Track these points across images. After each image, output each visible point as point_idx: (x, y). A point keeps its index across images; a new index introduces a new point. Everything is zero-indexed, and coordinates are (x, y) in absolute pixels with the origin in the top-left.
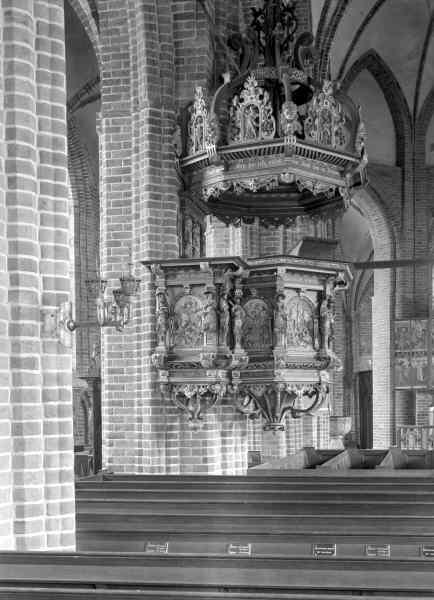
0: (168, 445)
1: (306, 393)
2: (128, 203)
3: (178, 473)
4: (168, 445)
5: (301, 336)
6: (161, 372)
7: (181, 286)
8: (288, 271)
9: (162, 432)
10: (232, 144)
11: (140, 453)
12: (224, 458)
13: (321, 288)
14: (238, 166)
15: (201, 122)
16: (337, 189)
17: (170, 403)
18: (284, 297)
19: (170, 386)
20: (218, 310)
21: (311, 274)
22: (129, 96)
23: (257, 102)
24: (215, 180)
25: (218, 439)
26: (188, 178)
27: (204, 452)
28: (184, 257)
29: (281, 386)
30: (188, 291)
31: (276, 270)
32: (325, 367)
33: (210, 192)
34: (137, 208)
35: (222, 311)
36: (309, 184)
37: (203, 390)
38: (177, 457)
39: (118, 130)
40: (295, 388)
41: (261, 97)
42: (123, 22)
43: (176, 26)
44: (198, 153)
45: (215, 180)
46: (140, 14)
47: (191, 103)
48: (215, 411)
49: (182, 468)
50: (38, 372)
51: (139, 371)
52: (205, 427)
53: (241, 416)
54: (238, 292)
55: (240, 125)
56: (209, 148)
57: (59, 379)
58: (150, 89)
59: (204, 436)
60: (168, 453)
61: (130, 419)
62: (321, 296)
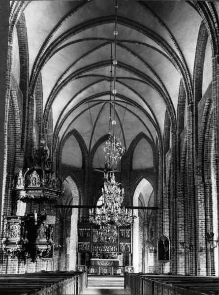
5: (44, 236)
6: (4, 245)
12: (18, 270)
14: (30, 192)
23: (36, 177)
24: (23, 194)
33: (21, 197)
36: (48, 197)
45: (23, 194)
56: (22, 187)
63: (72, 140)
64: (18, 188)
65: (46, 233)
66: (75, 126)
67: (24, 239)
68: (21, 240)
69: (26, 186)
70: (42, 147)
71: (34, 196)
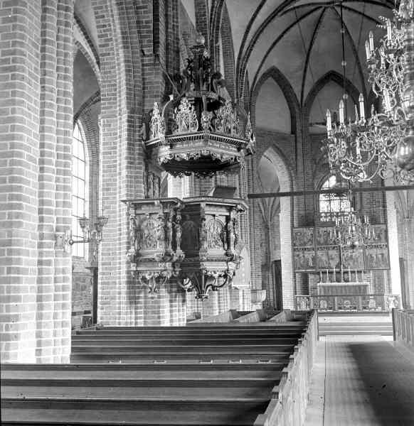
0: (136, 308)
1: (220, 276)
2: (115, 166)
3: (142, 326)
4: (136, 308)
5: (216, 242)
6: (132, 264)
7: (144, 214)
8: (207, 204)
9: (133, 300)
10: (174, 135)
11: (120, 313)
12: (171, 316)
13: (228, 214)
14: (178, 146)
15: (157, 121)
16: (235, 159)
17: (136, 284)
18: (205, 220)
19: (137, 273)
20: (166, 229)
21: (221, 206)
22: (116, 108)
24: (165, 153)
25: (168, 304)
26: (149, 153)
27: (159, 313)
28: (147, 197)
29: (204, 272)
30: (148, 217)
31: (200, 205)
32: (231, 260)
33: (162, 160)
34: (120, 169)
35: (168, 228)
36: (219, 156)
37: (156, 275)
38: (143, 315)
39: (110, 125)
40: (213, 273)
41: (190, 109)
42: (114, 67)
43: (143, 70)
44: (156, 138)
45: (165, 153)
46: (123, 64)
47: (152, 111)
48: (165, 287)
49: (145, 322)
50: (52, 267)
51: (120, 263)
52: (159, 297)
53: (182, 291)
54: (179, 217)
55: (179, 124)
57: (64, 271)
58: (128, 103)
59: (158, 302)
60: (136, 313)
61: (114, 293)
62: (228, 219)
63: (271, 87)
64: (153, 140)
65: (221, 235)
66: (273, 61)
67: (174, 248)
68: (167, 254)
69: (169, 132)
70: (199, 50)
71: (188, 155)
